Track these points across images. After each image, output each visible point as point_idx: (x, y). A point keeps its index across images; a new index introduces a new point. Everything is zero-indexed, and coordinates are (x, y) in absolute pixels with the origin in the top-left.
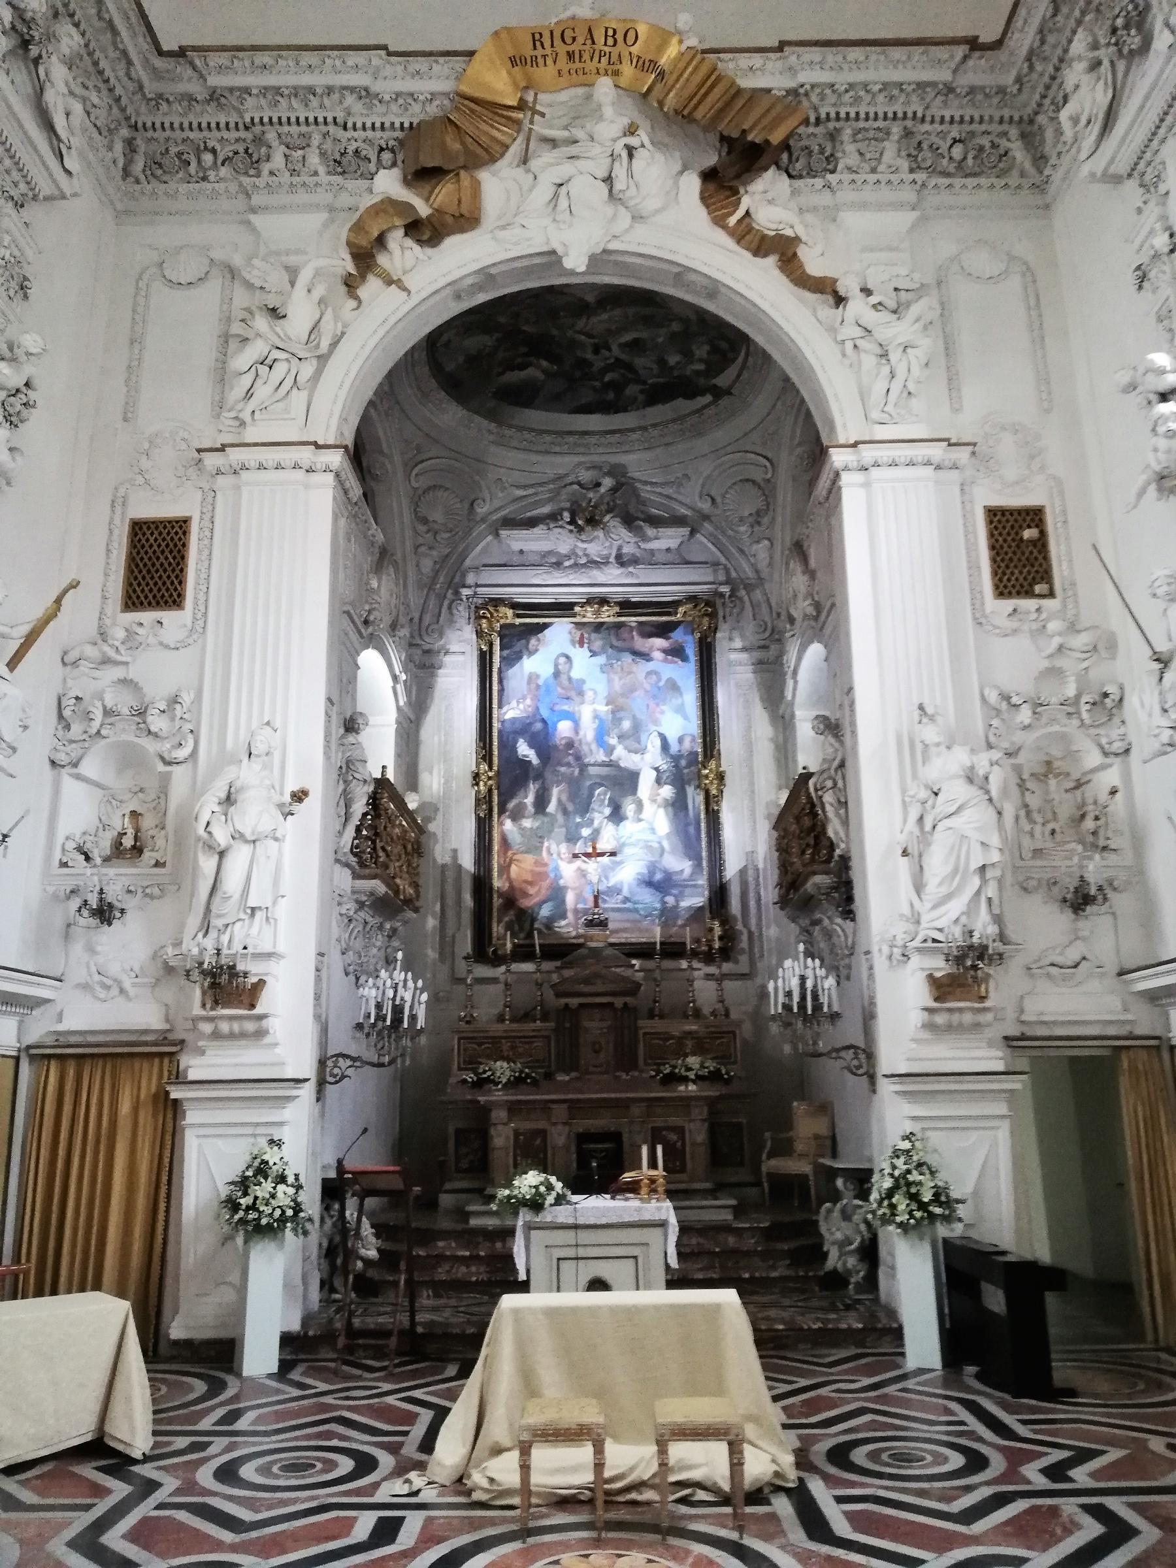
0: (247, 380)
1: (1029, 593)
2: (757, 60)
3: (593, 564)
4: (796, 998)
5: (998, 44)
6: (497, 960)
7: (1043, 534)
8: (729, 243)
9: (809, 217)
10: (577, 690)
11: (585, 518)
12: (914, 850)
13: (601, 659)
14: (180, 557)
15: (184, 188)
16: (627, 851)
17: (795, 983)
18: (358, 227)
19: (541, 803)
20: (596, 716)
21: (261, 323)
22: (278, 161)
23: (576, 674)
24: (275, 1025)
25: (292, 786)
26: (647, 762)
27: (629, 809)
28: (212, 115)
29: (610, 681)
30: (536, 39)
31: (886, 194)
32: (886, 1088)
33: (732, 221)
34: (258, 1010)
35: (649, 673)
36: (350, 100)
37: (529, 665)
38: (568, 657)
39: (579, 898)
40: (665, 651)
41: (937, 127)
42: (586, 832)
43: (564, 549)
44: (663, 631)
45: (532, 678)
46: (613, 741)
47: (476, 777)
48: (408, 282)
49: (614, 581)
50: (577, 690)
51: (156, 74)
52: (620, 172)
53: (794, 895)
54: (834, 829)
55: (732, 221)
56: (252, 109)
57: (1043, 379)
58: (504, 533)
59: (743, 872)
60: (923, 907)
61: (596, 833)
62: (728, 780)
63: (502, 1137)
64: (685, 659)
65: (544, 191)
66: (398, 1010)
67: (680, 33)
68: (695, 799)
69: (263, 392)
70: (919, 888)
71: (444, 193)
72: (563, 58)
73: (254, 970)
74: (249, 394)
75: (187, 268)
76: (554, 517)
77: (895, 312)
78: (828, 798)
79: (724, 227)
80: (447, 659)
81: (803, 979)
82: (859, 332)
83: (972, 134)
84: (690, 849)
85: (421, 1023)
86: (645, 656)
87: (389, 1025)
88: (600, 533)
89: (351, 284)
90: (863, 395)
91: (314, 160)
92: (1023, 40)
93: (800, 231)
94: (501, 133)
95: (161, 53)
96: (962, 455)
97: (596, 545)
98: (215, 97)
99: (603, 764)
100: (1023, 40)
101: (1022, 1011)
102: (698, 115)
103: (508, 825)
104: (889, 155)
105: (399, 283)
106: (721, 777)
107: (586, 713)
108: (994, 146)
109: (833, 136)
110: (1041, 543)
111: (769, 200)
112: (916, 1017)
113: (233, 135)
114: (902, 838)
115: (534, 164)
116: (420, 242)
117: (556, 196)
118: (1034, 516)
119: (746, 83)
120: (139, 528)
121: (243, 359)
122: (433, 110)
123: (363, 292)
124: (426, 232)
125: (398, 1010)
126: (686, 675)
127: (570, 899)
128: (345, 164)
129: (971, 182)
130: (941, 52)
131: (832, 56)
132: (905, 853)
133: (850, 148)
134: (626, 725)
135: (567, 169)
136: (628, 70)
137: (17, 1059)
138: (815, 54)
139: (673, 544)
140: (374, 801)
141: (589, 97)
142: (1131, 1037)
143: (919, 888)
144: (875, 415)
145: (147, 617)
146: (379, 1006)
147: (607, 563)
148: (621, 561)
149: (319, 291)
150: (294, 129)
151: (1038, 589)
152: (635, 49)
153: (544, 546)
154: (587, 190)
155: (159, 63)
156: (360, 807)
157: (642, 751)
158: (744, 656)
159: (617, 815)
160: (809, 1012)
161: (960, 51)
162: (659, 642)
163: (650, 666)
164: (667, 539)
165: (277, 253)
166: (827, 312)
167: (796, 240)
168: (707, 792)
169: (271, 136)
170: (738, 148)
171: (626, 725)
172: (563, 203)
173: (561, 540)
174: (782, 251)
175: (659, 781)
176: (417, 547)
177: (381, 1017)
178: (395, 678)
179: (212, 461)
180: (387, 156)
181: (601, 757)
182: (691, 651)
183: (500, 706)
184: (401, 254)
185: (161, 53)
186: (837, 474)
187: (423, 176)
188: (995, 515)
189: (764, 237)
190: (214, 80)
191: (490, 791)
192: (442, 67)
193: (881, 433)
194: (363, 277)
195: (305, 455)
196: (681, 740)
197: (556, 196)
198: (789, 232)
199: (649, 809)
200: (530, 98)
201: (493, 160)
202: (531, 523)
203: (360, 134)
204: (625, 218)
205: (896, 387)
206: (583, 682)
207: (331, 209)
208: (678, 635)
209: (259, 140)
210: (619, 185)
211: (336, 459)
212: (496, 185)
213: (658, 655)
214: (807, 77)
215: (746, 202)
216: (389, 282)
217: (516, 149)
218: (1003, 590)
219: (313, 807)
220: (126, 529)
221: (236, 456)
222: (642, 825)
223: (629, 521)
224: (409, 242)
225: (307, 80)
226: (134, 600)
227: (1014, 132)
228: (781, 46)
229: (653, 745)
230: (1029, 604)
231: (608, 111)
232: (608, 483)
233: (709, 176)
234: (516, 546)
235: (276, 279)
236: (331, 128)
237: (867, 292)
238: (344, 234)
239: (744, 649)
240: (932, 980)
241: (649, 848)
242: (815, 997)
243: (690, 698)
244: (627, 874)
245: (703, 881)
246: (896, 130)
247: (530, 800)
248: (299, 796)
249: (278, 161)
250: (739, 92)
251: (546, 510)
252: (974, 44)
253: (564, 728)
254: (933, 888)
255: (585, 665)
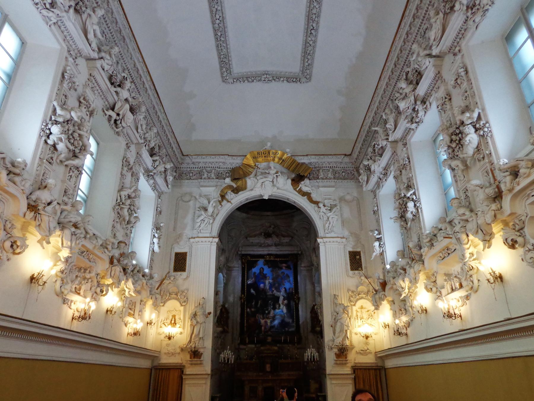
0: (199, 224)
1: (357, 269)
2: (302, 157)
3: (269, 246)
4: (310, 357)
5: (350, 155)
6: (245, 344)
7: (360, 257)
8: (297, 193)
9: (313, 188)
10: (265, 277)
11: (268, 235)
12: (333, 326)
13: (271, 269)
14: (185, 259)
15: (187, 181)
16: (277, 317)
17: (309, 354)
18: (222, 191)
19: (257, 303)
20: (269, 283)
21: (203, 212)
22: (206, 176)
23: (265, 272)
24: (204, 362)
25: (207, 311)
26: (281, 295)
27: (277, 306)
28: (192, 166)
29: (273, 275)
30: (258, 153)
31: (328, 184)
32: (327, 377)
33: (298, 189)
34: (201, 359)
35: (282, 272)
36: (221, 164)
37: (254, 270)
38: (263, 268)
39: (265, 328)
40: (286, 267)
41: (339, 169)
42: (266, 312)
43: (262, 242)
44: (285, 262)
45: (255, 273)
46: (273, 289)
47: (241, 298)
48: (232, 201)
49: (273, 250)
50: (265, 277)
51: (182, 159)
52: (275, 180)
53: (313, 331)
54: (320, 318)
55: (298, 189)
56: (200, 165)
57: (361, 223)
58: (248, 238)
59: (303, 322)
60: (334, 338)
61: (269, 313)
62: (301, 299)
63: (247, 389)
64: (291, 269)
65: (259, 184)
66: (228, 359)
67: (287, 153)
68: (293, 304)
69: (202, 225)
70: (334, 333)
71: (240, 183)
72: (263, 157)
73: (201, 350)
74: (200, 226)
75: (187, 198)
76: (261, 234)
77: (330, 210)
78: (319, 311)
79: (296, 191)
80: (235, 269)
81: (311, 353)
82: (323, 214)
83: (346, 170)
84: (292, 317)
85: (232, 362)
86: (281, 268)
87: (226, 363)
88: (271, 239)
89: (220, 202)
90: (324, 226)
91: (213, 175)
92: (355, 156)
93: (311, 191)
94: (251, 170)
95: (183, 155)
96: (344, 240)
97: (269, 241)
98: (193, 163)
99: (271, 295)
100: (355, 156)
101: (355, 360)
102: (291, 169)
103: (248, 310)
104: (330, 175)
105: (230, 202)
106: (299, 299)
107: (267, 282)
108: (351, 173)
109: (318, 170)
110: (360, 259)
111: (305, 185)
112: (333, 362)
113: (196, 169)
114: (331, 323)
115: (258, 178)
116: (234, 193)
117: (262, 185)
118: (358, 253)
119: (299, 161)
120: (177, 254)
121: (199, 220)
122: (237, 165)
123: (222, 204)
124: (236, 191)
125: (228, 359)
126: (290, 273)
127: (263, 328)
128: (219, 176)
129: (346, 181)
130: (339, 156)
131: (317, 157)
132: (332, 326)
133: (322, 173)
134: (277, 285)
135: (264, 180)
136: (276, 160)
137: (151, 369)
138: (313, 157)
139: (288, 241)
140: (221, 310)
141: (269, 164)
142: (377, 366)
143: (334, 333)
144: (326, 231)
145: (179, 273)
146: (224, 358)
147: (272, 245)
148: (276, 245)
149: (214, 205)
150: (209, 169)
151: (360, 269)
152: (278, 156)
153: (257, 241)
154: (268, 184)
155: (182, 157)
156: (218, 312)
157: (280, 292)
158: (305, 268)
159: (274, 308)
160: (312, 360)
161: (343, 156)
162: (284, 265)
163: (282, 271)
164: (286, 240)
165: (205, 195)
166: (316, 208)
167: (310, 194)
168: (295, 302)
169: (204, 171)
170: (299, 174)
171: (277, 285)
172: (263, 186)
173: (262, 240)
174: (307, 195)
175: (284, 300)
176: (228, 242)
177: (225, 361)
178: (224, 277)
179: (192, 240)
180: (227, 174)
181: (270, 293)
182: (292, 267)
183: (247, 280)
184: (230, 195)
185: (183, 155)
186: (319, 244)
187: (234, 179)
188: (350, 252)
189: (304, 192)
190: (193, 160)
191: (244, 302)
192: (239, 158)
193: (327, 235)
194: (222, 200)
195: (211, 239)
196: (289, 289)
197: (262, 185)
198: (309, 192)
199: (282, 306)
200: (257, 164)
201: (249, 175)
202: (255, 236)
203: (222, 169)
204: (275, 189)
205: (330, 226)
206: (266, 274)
207: (216, 186)
208: (290, 263)
209: (202, 171)
210: (275, 182)
211: (217, 240)
212: (250, 182)
213: (284, 268)
214: (312, 161)
215: (300, 185)
216: (228, 201)
217: (254, 173)
218: (352, 269)
219: (211, 317)
220: (174, 254)
221: (197, 239)
222: (280, 310)
223: (277, 236)
224: (232, 193)
225: (212, 160)
226: (176, 270)
227: (355, 170)
228: (307, 155)
229: (283, 290)
230: (356, 272)
231: (272, 168)
232: (273, 226)
233: (293, 180)
234: (251, 241)
235: (206, 202)
236: (217, 169)
237: (324, 206)
238: (219, 192)
239: (305, 267)
240: (336, 354)
241: (281, 316)
242: (314, 357)
243: (292, 279)
244: (276, 322)
245: (294, 324)
246: (331, 170)
247: (253, 304)
248: (209, 313)
249: (206, 176)
250: (299, 163)
251: (258, 232)
252: (345, 155)
253: (262, 285)
254: (337, 335)
255: (267, 270)
